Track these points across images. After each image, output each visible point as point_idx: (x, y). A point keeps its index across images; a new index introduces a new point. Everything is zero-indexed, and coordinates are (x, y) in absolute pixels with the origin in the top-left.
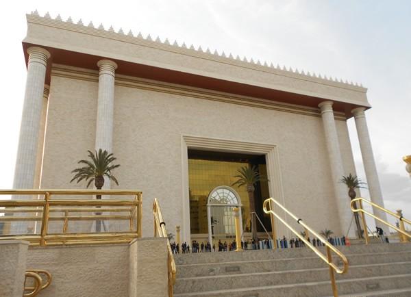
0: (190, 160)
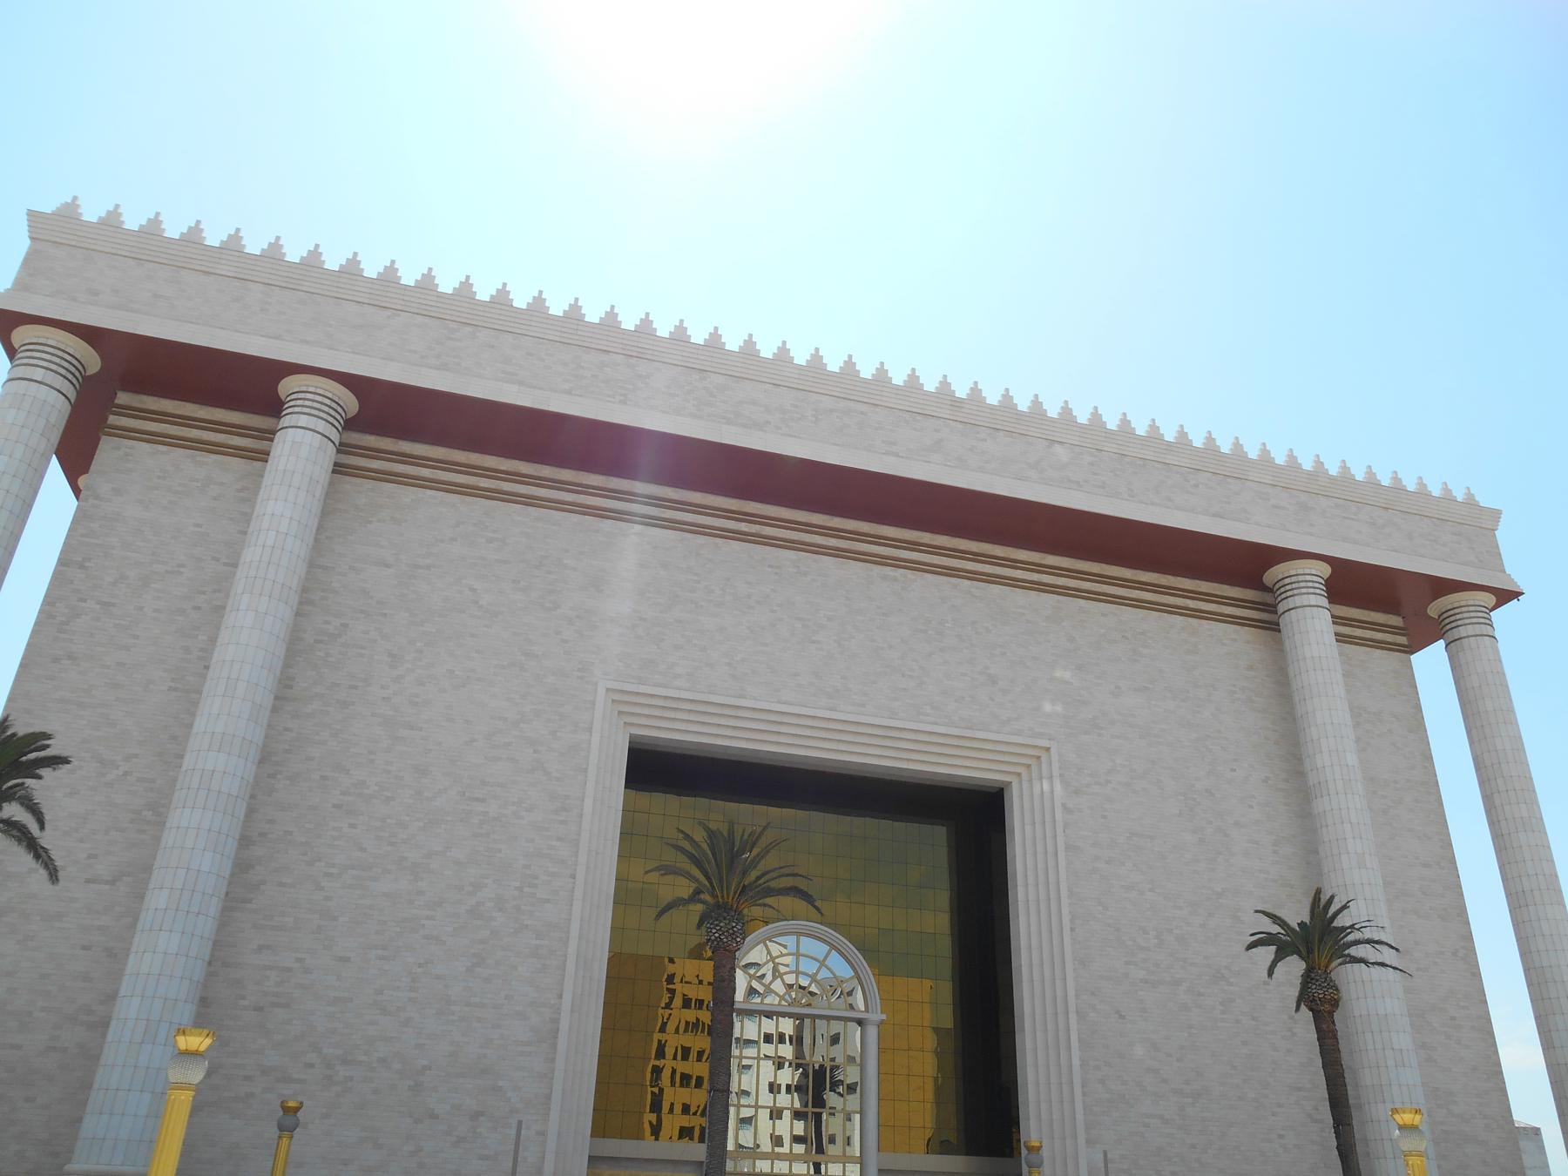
0: (644, 799)
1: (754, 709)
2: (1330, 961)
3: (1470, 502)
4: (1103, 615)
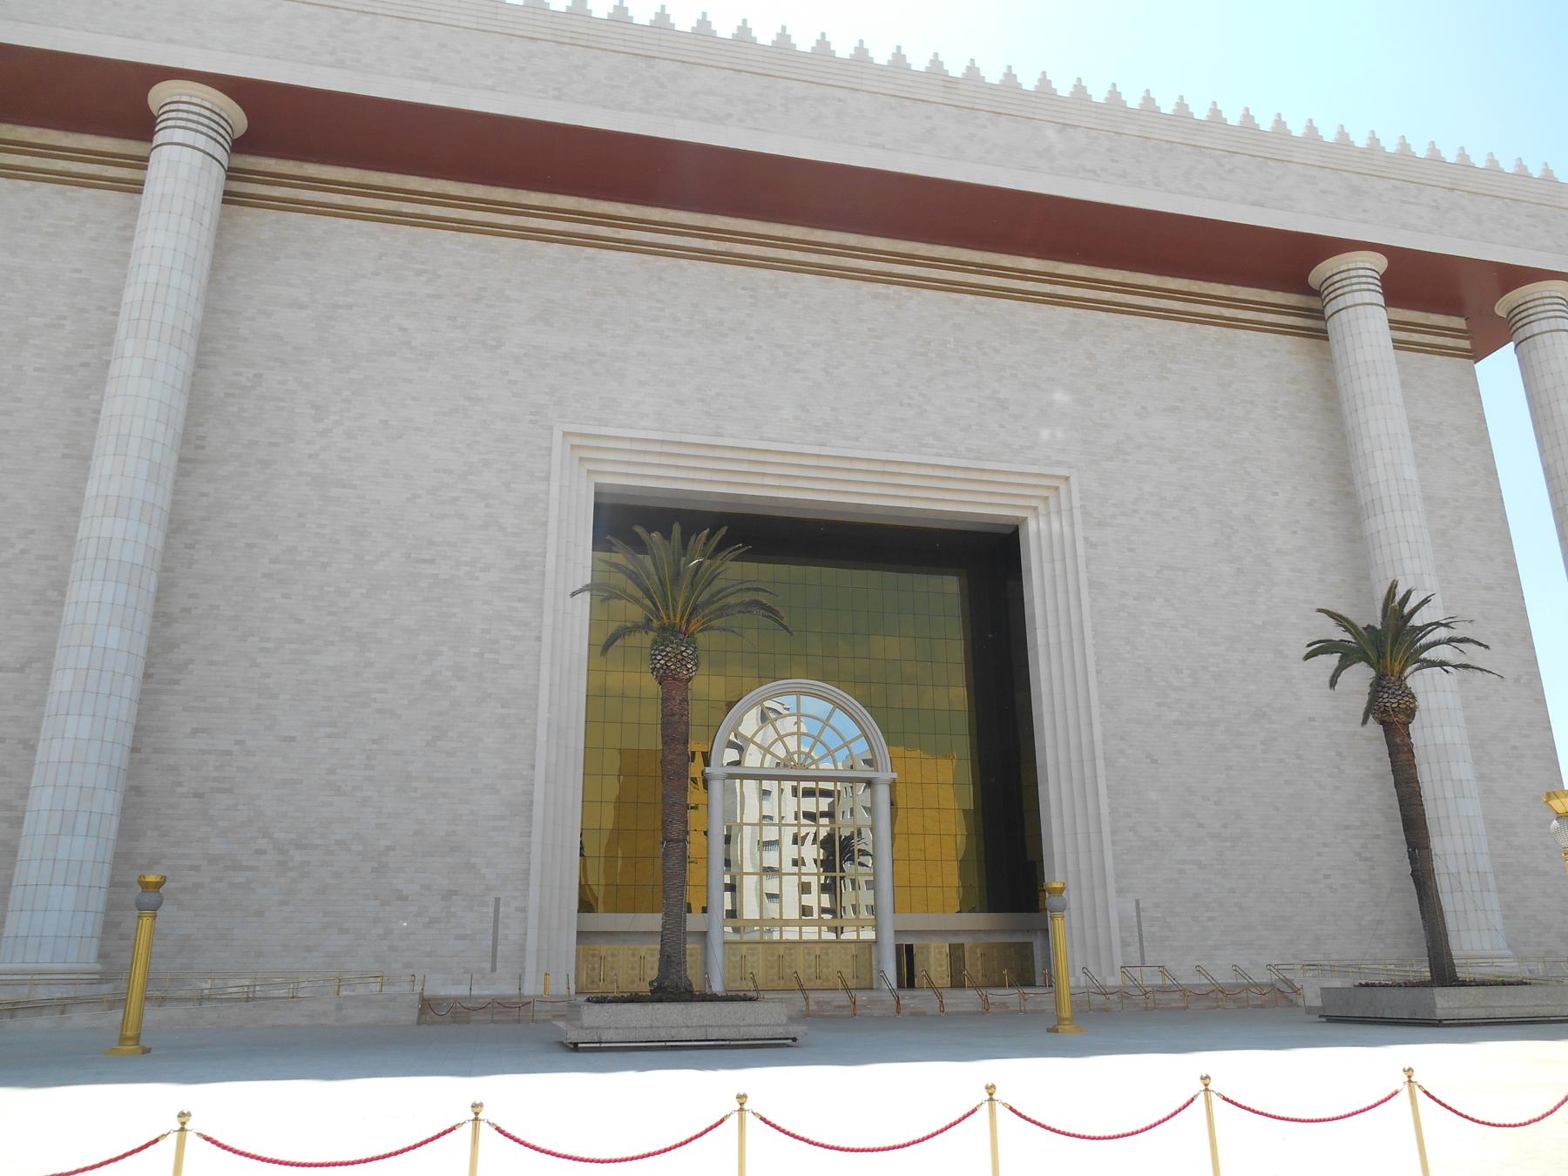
1: (733, 448)
2: (1401, 672)
3: (1548, 178)
4: (1128, 328)
